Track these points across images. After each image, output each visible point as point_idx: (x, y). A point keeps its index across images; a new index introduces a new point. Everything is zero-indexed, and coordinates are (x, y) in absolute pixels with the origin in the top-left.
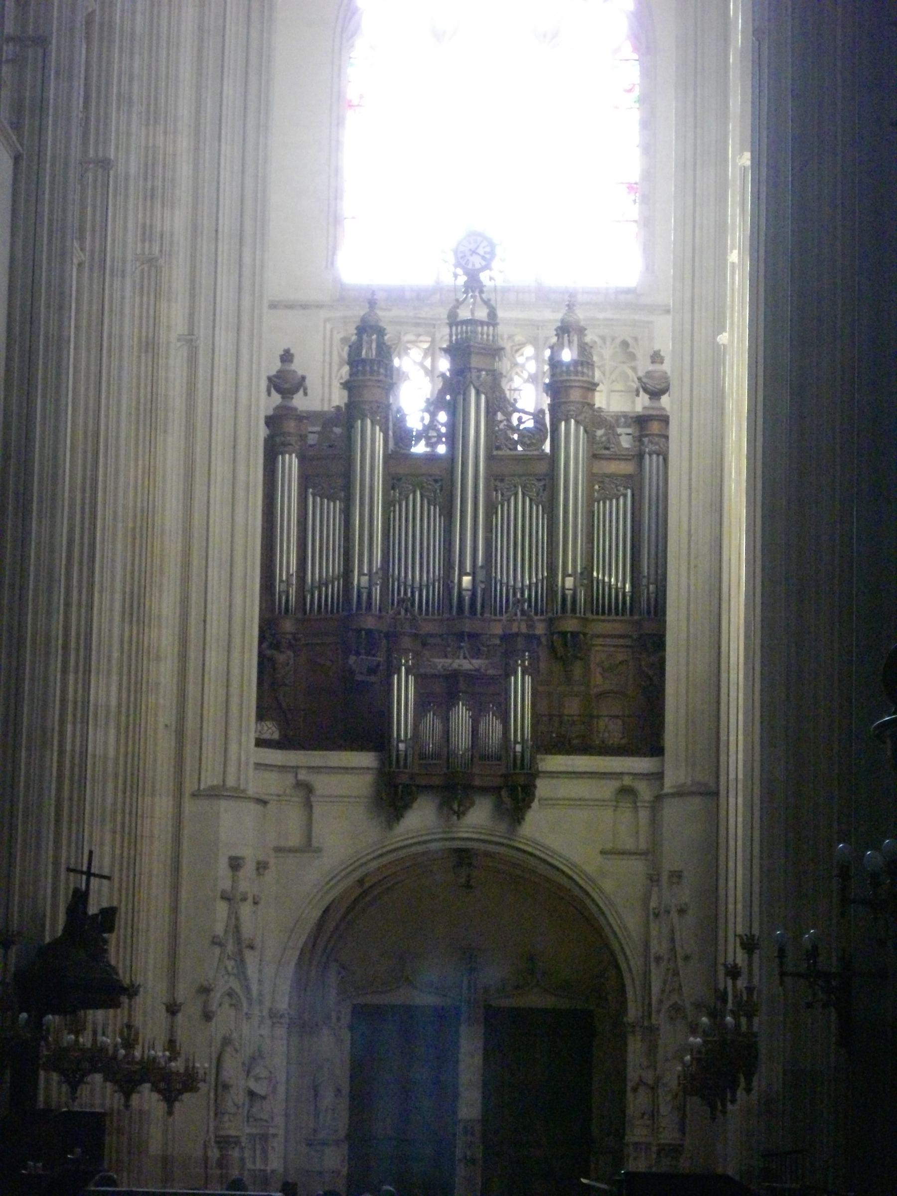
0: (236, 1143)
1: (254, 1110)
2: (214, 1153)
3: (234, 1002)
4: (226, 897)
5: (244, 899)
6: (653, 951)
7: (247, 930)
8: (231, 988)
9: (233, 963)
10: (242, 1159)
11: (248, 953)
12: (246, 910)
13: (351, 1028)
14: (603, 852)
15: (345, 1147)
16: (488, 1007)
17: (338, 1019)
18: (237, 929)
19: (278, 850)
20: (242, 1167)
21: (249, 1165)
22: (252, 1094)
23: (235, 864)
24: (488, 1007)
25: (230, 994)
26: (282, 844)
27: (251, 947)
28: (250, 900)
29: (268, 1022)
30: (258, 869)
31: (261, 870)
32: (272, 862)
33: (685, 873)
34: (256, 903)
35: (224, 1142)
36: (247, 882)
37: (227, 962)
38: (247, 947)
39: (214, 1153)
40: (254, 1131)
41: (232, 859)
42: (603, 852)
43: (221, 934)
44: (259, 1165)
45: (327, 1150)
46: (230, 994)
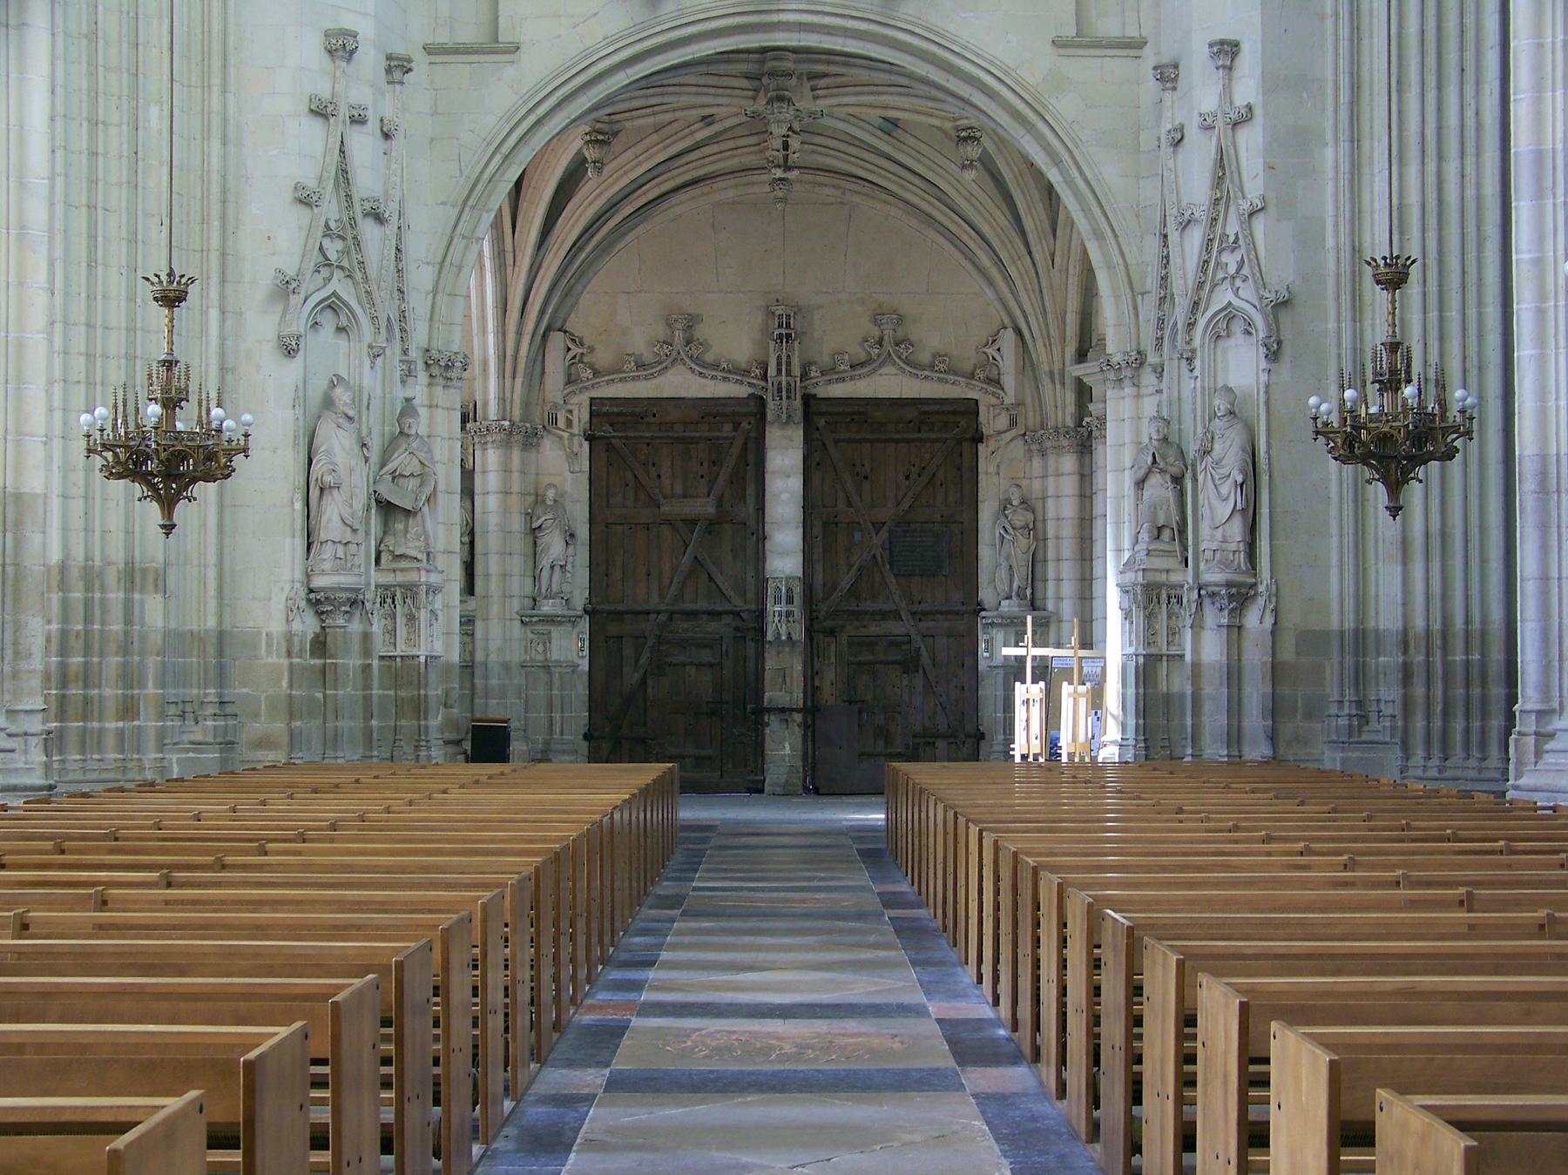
0: (353, 603)
1: (390, 541)
2: (307, 625)
3: (344, 322)
4: (321, 112)
5: (358, 120)
6: (1172, 212)
7: (366, 183)
8: (334, 294)
9: (339, 245)
10: (367, 637)
11: (368, 229)
12: (363, 145)
13: (590, 438)
14: (1058, 43)
15: (585, 625)
16: (808, 399)
17: (569, 423)
18: (344, 174)
19: (430, 50)
20: (367, 652)
21: (380, 647)
22: (387, 509)
23: (341, 47)
24: (808, 399)
25: (333, 305)
26: (443, 38)
27: (379, 218)
28: (373, 126)
29: (422, 377)
30: (389, 71)
31: (397, 75)
32: (420, 63)
33: (1245, 47)
34: (387, 136)
35: (318, 602)
36: (362, 84)
37: (327, 243)
38: (366, 215)
39: (307, 625)
40: (388, 579)
41: (327, 34)
42: (1058, 43)
43: (312, 184)
44: (402, 649)
45: (556, 632)
46: (333, 305)
